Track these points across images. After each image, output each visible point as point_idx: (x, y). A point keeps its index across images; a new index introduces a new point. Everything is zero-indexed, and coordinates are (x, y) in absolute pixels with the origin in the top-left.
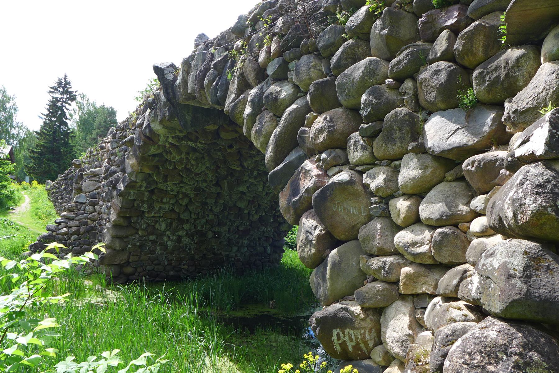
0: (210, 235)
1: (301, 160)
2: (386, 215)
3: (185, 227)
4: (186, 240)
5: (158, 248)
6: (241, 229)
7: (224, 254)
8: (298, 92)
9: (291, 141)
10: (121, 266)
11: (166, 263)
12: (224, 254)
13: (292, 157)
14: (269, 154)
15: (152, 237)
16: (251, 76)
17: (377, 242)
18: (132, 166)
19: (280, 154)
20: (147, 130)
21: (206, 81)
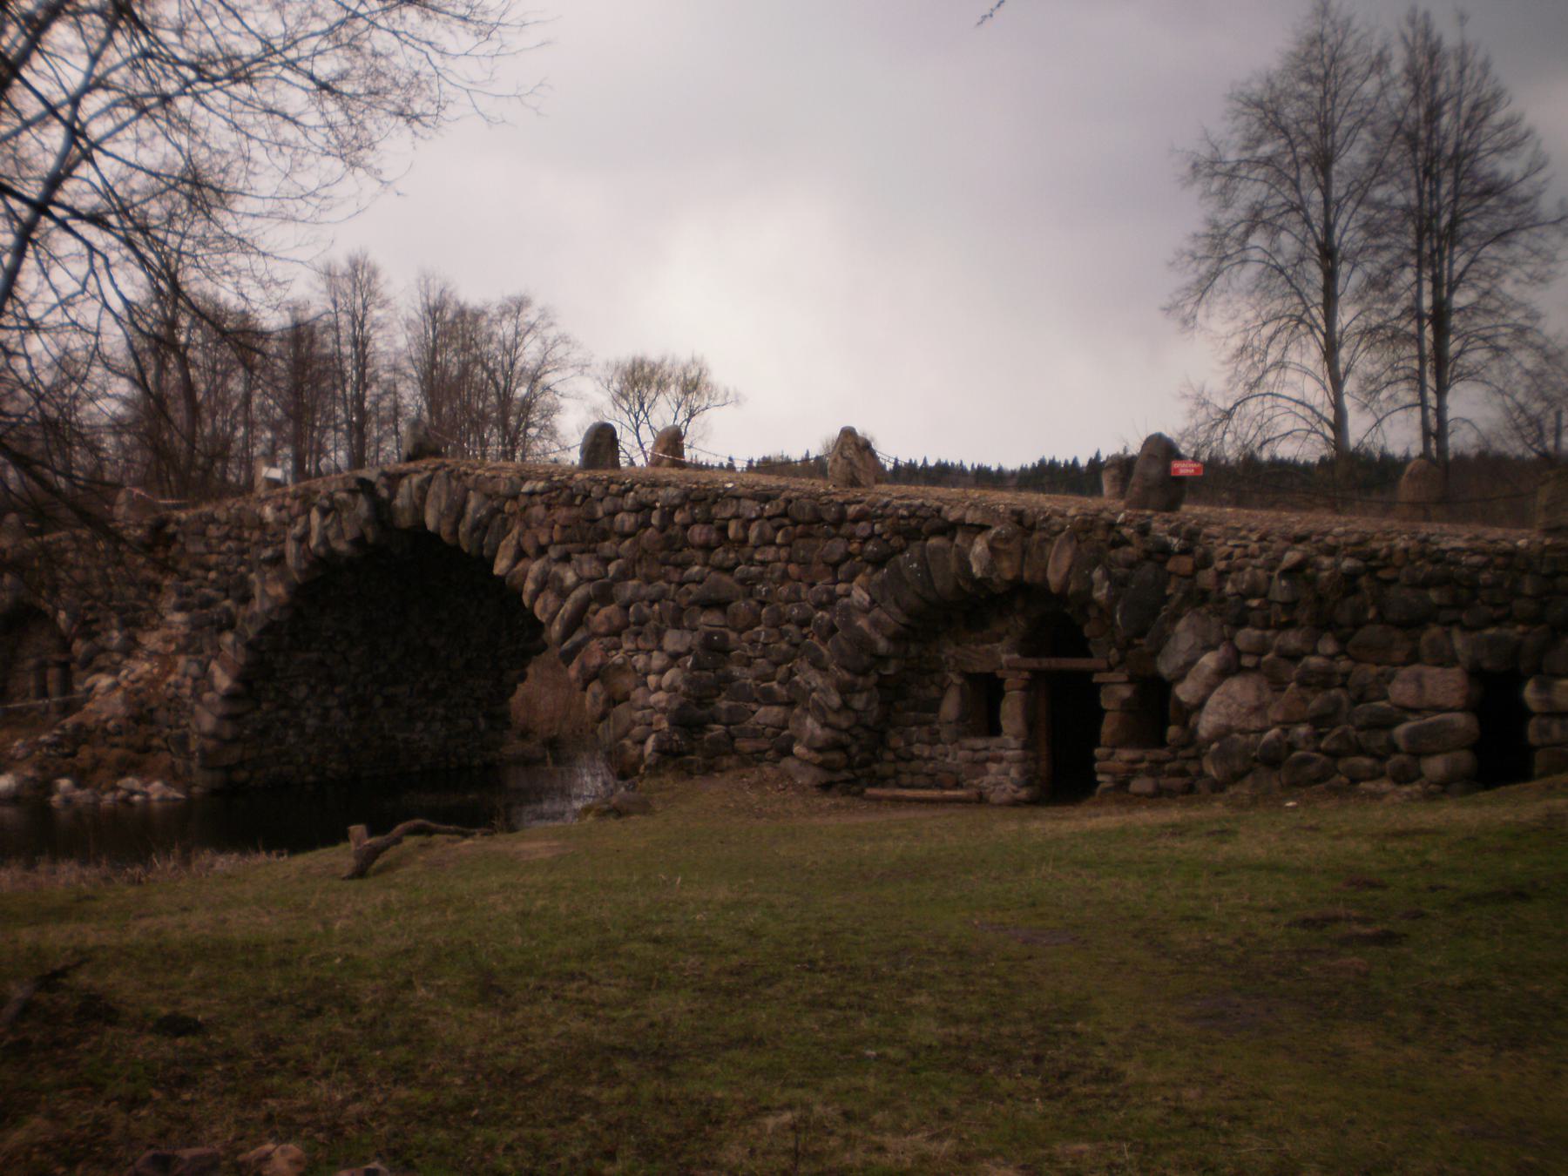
0: (378, 701)
1: (586, 641)
2: (645, 684)
3: (338, 690)
4: (337, 714)
5: (291, 732)
6: (433, 686)
7: (400, 736)
8: (580, 581)
9: (577, 620)
10: (228, 769)
11: (302, 759)
12: (400, 736)
13: (578, 636)
14: (556, 629)
15: (283, 714)
16: (531, 551)
17: (640, 703)
18: (277, 598)
19: (567, 633)
20: (322, 550)
21: (462, 529)
